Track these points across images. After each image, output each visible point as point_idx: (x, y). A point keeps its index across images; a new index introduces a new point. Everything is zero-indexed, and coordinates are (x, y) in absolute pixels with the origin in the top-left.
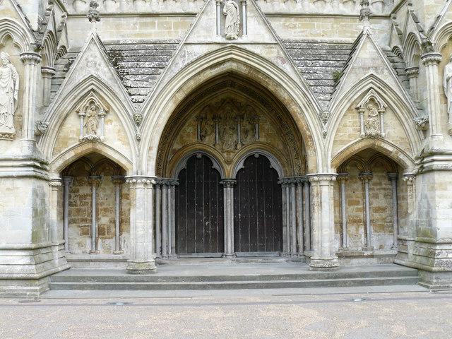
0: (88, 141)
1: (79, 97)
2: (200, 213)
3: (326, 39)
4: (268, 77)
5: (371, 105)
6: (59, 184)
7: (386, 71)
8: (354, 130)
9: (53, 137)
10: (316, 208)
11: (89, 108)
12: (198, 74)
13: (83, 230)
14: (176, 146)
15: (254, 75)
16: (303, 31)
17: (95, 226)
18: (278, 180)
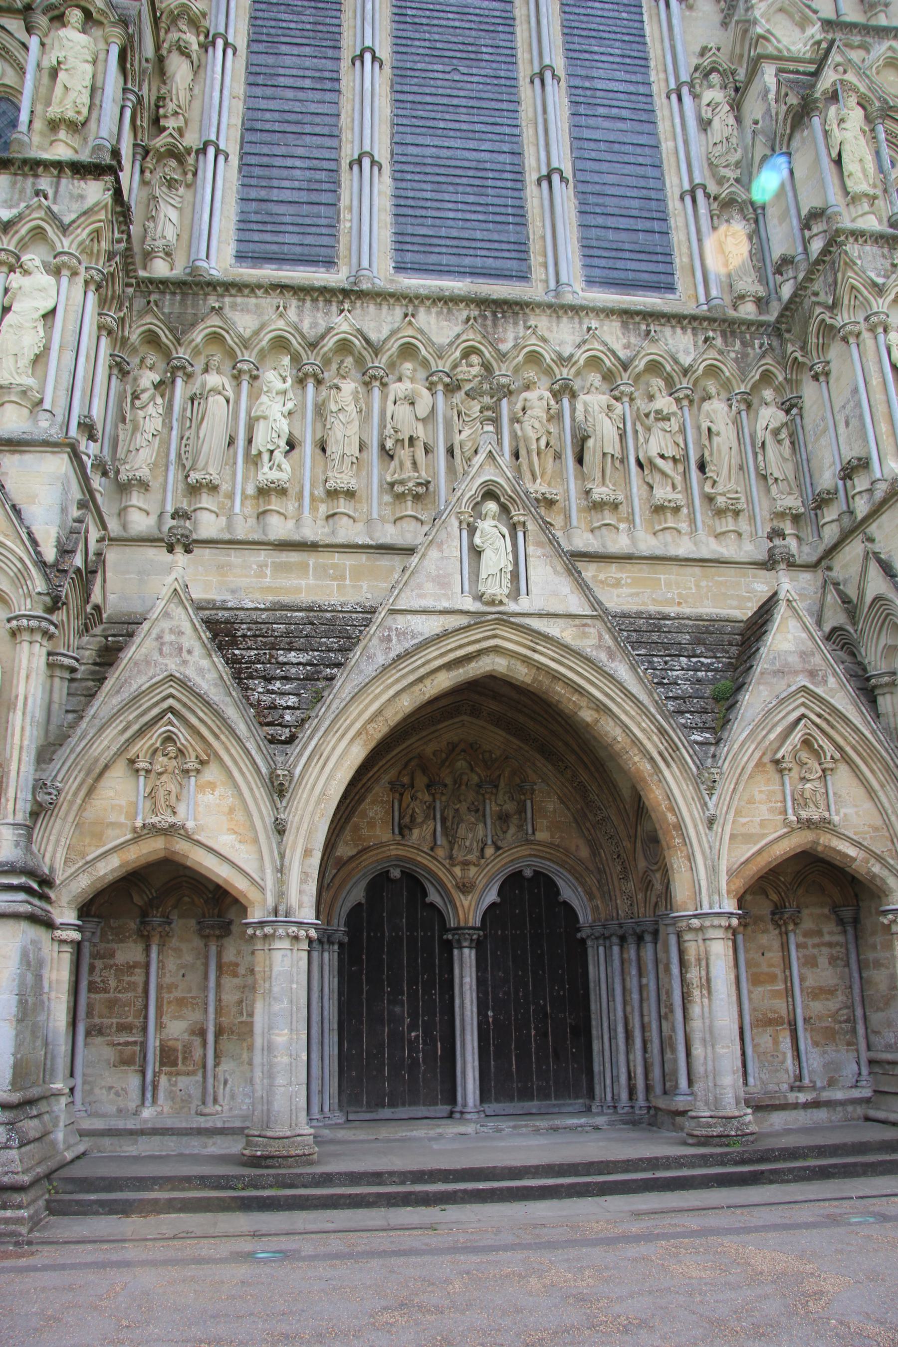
0: (155, 830)
1: (136, 727)
2: (398, 1009)
3: (687, 610)
5: (804, 755)
6: (76, 936)
7: (832, 681)
8: (771, 810)
9: (71, 818)
10: (696, 993)
11: (159, 753)
12: (420, 679)
13: (121, 1052)
14: (344, 850)
16: (637, 594)
17: (153, 1043)
18: (579, 930)
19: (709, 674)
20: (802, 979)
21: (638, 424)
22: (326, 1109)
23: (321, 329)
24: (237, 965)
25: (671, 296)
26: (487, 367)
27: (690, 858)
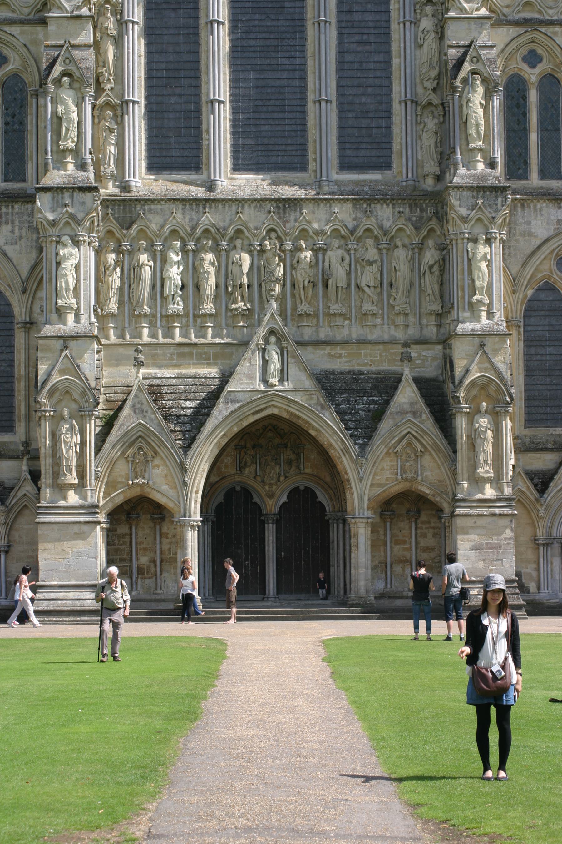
2: (239, 551)
3: (373, 368)
4: (307, 422)
8: (391, 473)
10: (353, 548)
15: (294, 420)
16: (350, 361)
18: (326, 515)
19: (376, 406)
20: (417, 543)
21: (358, 265)
22: (207, 595)
23: (195, 222)
24: (168, 534)
25: (389, 172)
26: (278, 238)
27: (352, 493)
